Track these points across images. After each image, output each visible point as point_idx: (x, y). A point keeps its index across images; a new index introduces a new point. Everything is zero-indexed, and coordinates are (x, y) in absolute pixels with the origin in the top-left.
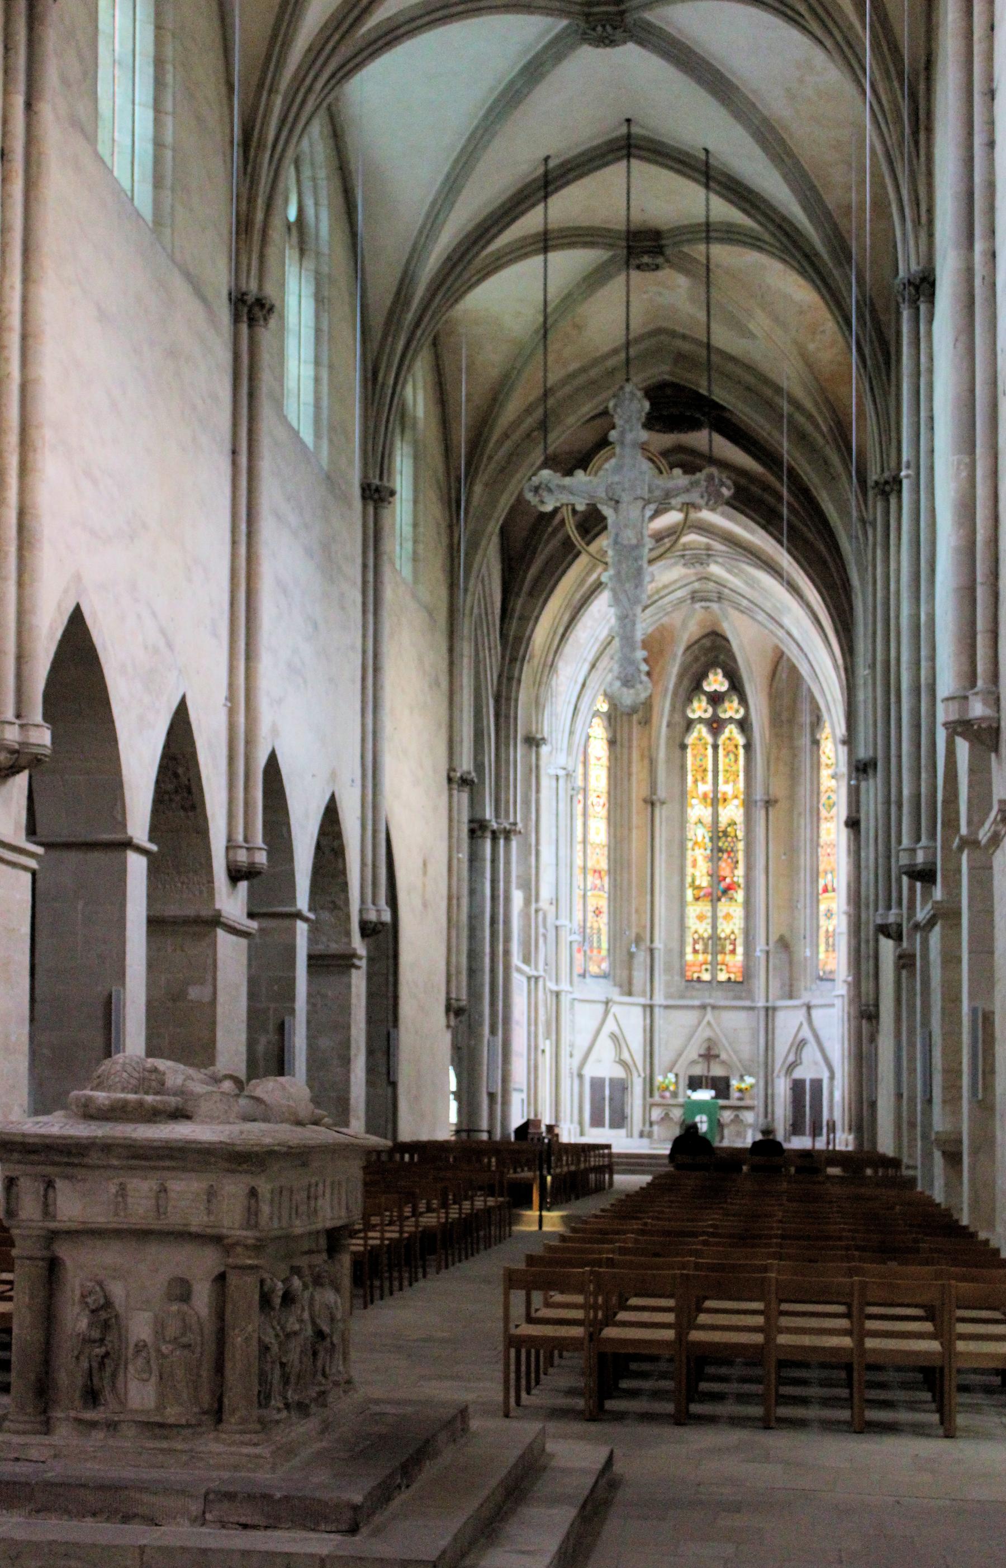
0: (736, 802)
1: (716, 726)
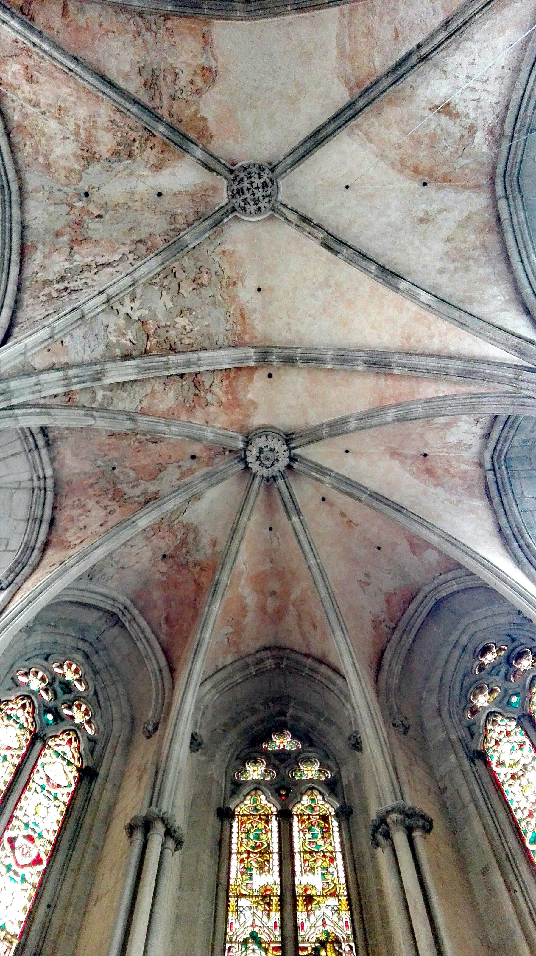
0: (333, 902)
1: (285, 790)
